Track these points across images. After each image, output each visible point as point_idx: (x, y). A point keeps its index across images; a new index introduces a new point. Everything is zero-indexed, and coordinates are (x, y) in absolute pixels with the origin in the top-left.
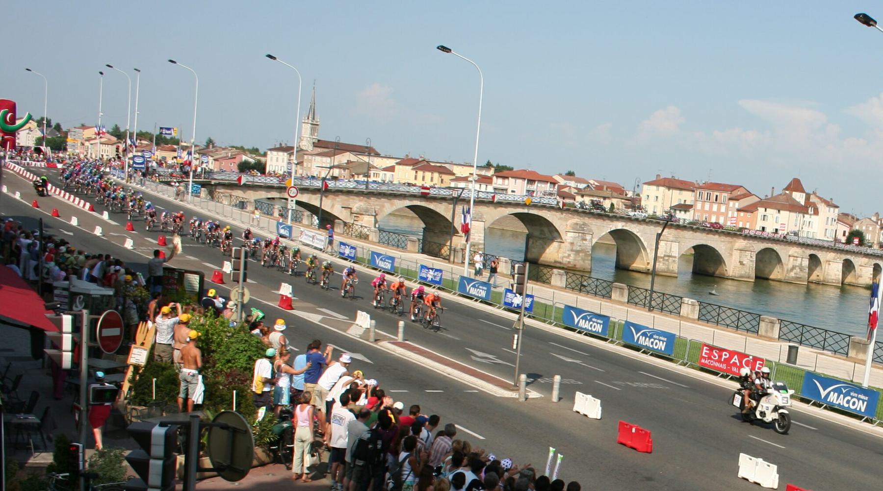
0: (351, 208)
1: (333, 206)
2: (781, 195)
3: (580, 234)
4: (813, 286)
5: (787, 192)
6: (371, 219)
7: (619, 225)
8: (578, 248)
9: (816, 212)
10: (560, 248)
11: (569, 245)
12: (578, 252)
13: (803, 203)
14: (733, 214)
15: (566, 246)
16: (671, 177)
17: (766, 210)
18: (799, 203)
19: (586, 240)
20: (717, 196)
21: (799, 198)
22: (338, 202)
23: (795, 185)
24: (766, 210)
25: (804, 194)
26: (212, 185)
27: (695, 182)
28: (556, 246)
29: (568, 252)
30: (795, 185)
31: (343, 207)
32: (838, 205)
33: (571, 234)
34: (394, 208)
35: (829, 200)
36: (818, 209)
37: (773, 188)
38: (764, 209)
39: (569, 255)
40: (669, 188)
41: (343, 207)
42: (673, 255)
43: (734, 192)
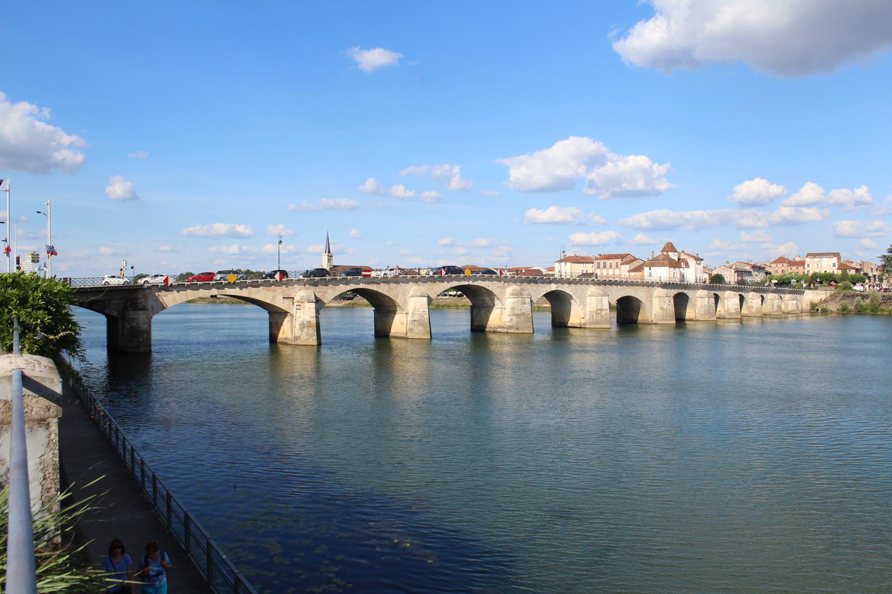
0: (293, 298)
1: (274, 297)
2: (660, 255)
3: (520, 299)
4: (720, 322)
5: (664, 253)
6: (312, 306)
7: (553, 287)
8: (519, 312)
9: (687, 265)
10: (502, 314)
11: (510, 310)
12: (518, 315)
13: (677, 260)
15: (508, 311)
17: (650, 269)
18: (674, 260)
19: (525, 303)
20: (611, 263)
21: (673, 256)
22: (279, 293)
23: (670, 247)
24: (650, 269)
25: (677, 253)
26: (146, 289)
27: (592, 257)
28: (499, 313)
29: (510, 317)
30: (670, 247)
31: (284, 298)
32: (702, 258)
33: (512, 300)
34: (337, 294)
35: (696, 256)
36: (688, 263)
37: (653, 252)
38: (648, 268)
39: (511, 320)
40: (574, 262)
41: (284, 298)
42: (604, 308)
43: (626, 259)
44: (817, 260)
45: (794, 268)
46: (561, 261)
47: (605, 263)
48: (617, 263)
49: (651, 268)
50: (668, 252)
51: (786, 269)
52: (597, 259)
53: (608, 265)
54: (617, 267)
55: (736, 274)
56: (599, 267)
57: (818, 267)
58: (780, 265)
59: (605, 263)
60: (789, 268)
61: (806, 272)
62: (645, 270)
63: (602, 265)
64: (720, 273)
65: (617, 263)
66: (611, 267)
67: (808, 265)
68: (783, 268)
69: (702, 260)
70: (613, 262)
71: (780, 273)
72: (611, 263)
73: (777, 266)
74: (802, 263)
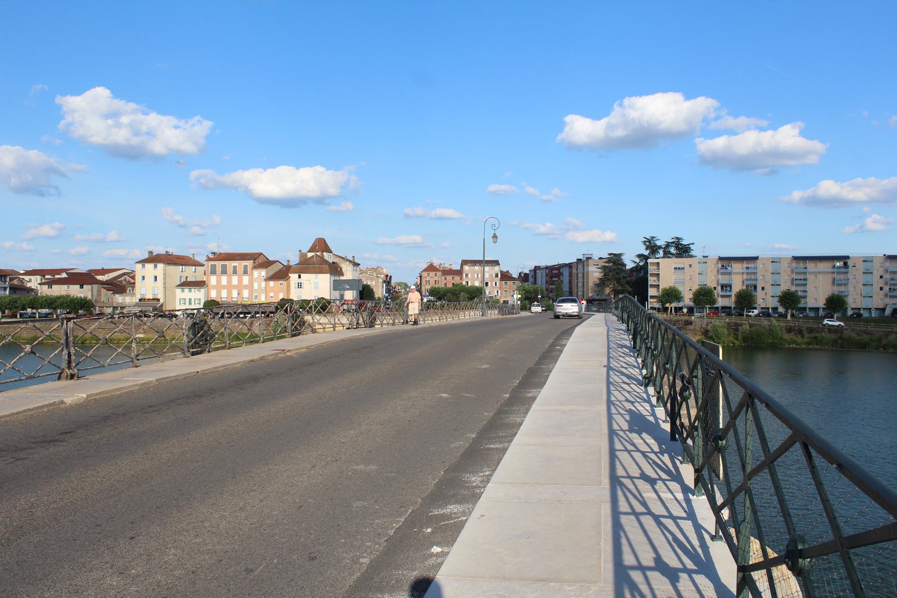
14: (259, 285)
16: (164, 253)
17: (300, 277)
20: (235, 267)
23: (321, 245)
24: (300, 277)
30: (321, 245)
38: (297, 275)
44: (477, 268)
45: (449, 278)
46: (144, 262)
47: (224, 267)
48: (246, 267)
49: (302, 275)
50: (323, 252)
51: (439, 279)
52: (209, 259)
53: (230, 270)
54: (245, 272)
55: (384, 284)
56: (213, 272)
57: (478, 277)
58: (432, 274)
59: (224, 267)
60: (443, 277)
61: (464, 283)
62: (291, 279)
63: (219, 269)
64: (369, 283)
65: (246, 267)
66: (235, 272)
67: (467, 275)
68: (436, 278)
69: (359, 265)
70: (239, 264)
71: (433, 284)
72: (235, 267)
73: (428, 274)
74: (459, 273)
